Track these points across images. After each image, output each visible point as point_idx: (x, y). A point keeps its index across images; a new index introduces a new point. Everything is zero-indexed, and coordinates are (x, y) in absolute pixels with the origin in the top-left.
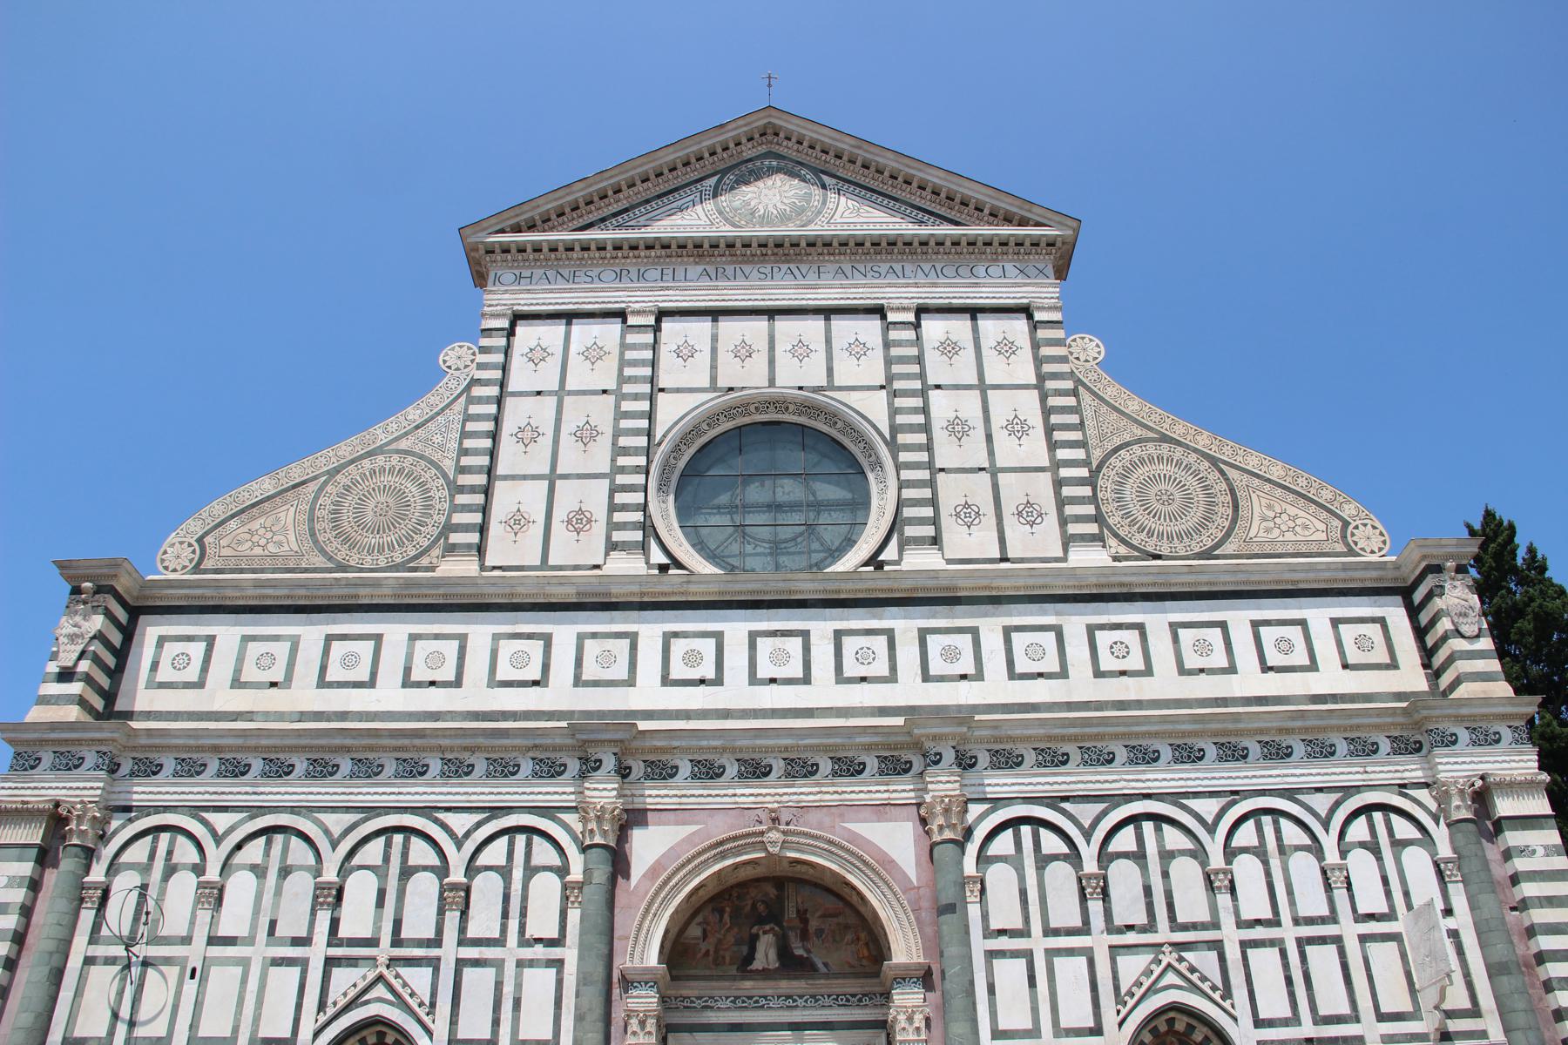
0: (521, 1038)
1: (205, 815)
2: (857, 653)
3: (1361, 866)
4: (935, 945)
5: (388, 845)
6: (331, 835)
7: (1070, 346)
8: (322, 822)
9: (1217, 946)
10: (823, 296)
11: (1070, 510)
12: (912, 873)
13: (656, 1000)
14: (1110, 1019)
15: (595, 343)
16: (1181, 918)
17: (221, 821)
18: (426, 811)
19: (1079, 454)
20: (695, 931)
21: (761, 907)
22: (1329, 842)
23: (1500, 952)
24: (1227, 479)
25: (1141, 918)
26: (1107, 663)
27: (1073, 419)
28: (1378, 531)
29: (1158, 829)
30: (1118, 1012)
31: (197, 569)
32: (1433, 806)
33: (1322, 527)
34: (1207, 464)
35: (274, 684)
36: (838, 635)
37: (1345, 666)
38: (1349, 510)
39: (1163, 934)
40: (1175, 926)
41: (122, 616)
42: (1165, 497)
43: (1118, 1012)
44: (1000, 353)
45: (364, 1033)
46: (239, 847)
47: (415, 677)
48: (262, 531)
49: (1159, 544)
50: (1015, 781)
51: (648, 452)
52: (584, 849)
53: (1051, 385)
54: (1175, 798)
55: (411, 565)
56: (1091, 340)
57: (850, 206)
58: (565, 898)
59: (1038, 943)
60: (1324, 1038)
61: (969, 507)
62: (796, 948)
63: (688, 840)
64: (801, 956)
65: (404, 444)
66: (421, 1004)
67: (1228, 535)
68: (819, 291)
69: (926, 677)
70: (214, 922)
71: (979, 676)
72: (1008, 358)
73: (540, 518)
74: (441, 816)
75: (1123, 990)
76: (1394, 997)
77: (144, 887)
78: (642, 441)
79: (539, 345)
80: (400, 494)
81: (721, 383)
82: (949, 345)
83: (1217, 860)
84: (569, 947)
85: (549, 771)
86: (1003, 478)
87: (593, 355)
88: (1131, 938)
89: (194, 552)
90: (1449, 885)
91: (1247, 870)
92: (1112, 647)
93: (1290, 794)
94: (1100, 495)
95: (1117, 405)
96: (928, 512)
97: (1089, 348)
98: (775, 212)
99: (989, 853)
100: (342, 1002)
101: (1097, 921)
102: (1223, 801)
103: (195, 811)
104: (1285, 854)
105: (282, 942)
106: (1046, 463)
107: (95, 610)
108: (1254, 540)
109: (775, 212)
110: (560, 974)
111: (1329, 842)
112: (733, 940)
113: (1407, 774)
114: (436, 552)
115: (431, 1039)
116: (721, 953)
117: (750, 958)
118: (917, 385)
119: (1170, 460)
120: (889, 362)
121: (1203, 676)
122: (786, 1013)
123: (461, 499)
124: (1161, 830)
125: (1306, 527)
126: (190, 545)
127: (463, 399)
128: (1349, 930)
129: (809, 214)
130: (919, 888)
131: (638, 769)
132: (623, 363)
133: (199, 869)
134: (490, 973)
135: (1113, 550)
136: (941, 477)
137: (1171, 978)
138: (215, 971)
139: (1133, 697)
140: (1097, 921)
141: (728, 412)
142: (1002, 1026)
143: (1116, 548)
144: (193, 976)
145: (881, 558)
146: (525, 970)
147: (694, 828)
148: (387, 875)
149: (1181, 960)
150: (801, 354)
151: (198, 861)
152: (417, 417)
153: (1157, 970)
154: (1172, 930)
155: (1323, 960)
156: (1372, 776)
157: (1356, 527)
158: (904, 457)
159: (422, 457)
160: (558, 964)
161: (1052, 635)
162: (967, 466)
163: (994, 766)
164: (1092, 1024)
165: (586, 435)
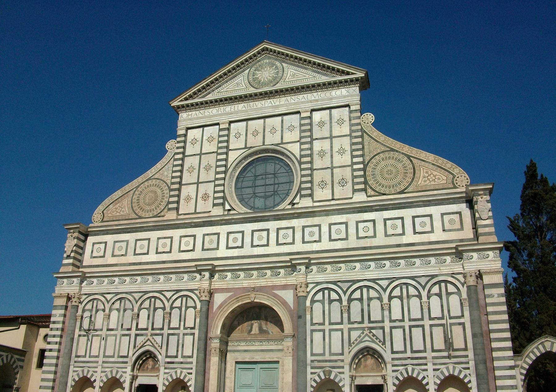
0: (184, 355)
1: (104, 295)
2: (283, 235)
3: (435, 302)
4: (296, 327)
5: (150, 302)
6: (136, 299)
7: (362, 118)
8: (133, 296)
9: (383, 328)
10: (281, 110)
11: (356, 180)
12: (292, 306)
13: (219, 344)
14: (346, 350)
15: (211, 136)
16: (372, 319)
17: (109, 297)
19: (361, 159)
21: (254, 315)
22: (424, 294)
23: (478, 330)
24: (412, 163)
25: (359, 319)
28: (466, 178)
29: (368, 291)
30: (349, 348)
31: (102, 221)
32: (462, 280)
33: (445, 178)
34: (406, 158)
35: (122, 255)
37: (444, 230)
39: (366, 324)
40: (370, 322)
41: (82, 237)
42: (389, 172)
43: (349, 348)
44: (338, 124)
45: (146, 354)
46: (113, 303)
47: (159, 251)
48: (119, 208)
49: (385, 190)
50: (323, 276)
51: (225, 172)
52: (201, 301)
54: (374, 281)
55: (158, 215)
56: (370, 115)
57: (292, 74)
58: (195, 315)
59: (327, 327)
60: (414, 357)
61: (323, 182)
62: (264, 327)
63: (230, 298)
64: (265, 330)
65: (156, 176)
66: (159, 346)
67: (410, 184)
68: (279, 108)
69: (304, 242)
70: (108, 324)
71: (320, 241)
72: (341, 125)
73: (195, 197)
74: (163, 293)
75: (352, 342)
76: (439, 343)
77: (91, 316)
78: (223, 169)
79: (194, 138)
80: (155, 192)
82: (321, 123)
83: (386, 300)
84: (196, 330)
85: (192, 278)
86: (335, 170)
88: (356, 325)
89: (101, 216)
90: (464, 307)
91: (396, 303)
92: (363, 228)
93: (412, 278)
94: (367, 173)
95: (376, 139)
96: (309, 185)
97: (370, 117)
98: (267, 80)
99: (314, 299)
100: (139, 346)
101: (345, 320)
102: (390, 281)
103: (102, 294)
104: (409, 298)
105: (124, 330)
106: (350, 164)
107: (74, 238)
108: (419, 185)
109: (267, 80)
110: (194, 337)
111: (424, 294)
112: (246, 325)
113: (455, 270)
114: (166, 210)
115: (161, 355)
116: (243, 329)
117: (251, 330)
118: (309, 139)
119: (393, 158)
120: (302, 131)
121: (393, 237)
122: (260, 347)
123: (172, 193)
124: (369, 291)
125: (439, 179)
126: (100, 214)
127: (173, 159)
128: (427, 323)
129: (278, 79)
130: (293, 310)
133: (104, 310)
134: (176, 337)
135: (369, 193)
136: (315, 172)
137: (367, 338)
138: (109, 338)
139: (368, 245)
140: (345, 320)
141: (250, 155)
142: (315, 352)
143: (370, 192)
144: (103, 340)
145: (294, 202)
146: (185, 336)
147: (231, 294)
148: (150, 310)
149: (371, 332)
150: (273, 132)
151: (104, 308)
152: (160, 167)
153: (362, 336)
154: (369, 323)
155: (417, 333)
156: (442, 271)
157: (458, 177)
158: (303, 166)
159: (161, 180)
160: (193, 334)
161: (344, 225)
162: (324, 167)
163: (318, 272)
164: (341, 352)
165: (208, 168)
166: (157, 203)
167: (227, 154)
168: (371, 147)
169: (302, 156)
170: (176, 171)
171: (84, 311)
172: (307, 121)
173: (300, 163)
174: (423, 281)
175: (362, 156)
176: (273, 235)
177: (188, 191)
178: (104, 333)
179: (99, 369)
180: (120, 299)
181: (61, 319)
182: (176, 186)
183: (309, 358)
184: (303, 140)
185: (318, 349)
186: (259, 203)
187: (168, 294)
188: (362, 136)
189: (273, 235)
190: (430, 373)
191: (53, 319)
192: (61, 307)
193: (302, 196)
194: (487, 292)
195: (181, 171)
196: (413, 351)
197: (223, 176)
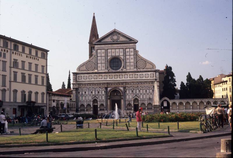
3: (148, 90)
17: (85, 88)
19: (136, 61)
22: (146, 89)
26: (135, 77)
27: (136, 58)
38: (154, 65)
47: (95, 78)
53: (135, 55)
59: (129, 94)
69: (124, 78)
73: (101, 66)
78: (107, 61)
80: (91, 65)
83: (139, 90)
87: (103, 53)
91: (141, 90)
93: (144, 86)
111: (146, 89)
120: (124, 53)
123: (96, 65)
128: (146, 94)
132: (105, 54)
136: (127, 63)
140: (132, 93)
155: (144, 96)
158: (124, 62)
166: (92, 67)
167: (107, 57)
168: (138, 59)
169: (124, 59)
172: (125, 51)
173: (123, 61)
175: (136, 60)
176: (118, 76)
177: (99, 65)
178: (85, 95)
179: (85, 104)
180: (88, 89)
181: (75, 93)
182: (96, 64)
183: (126, 100)
184: (124, 55)
185: (128, 98)
186: (115, 68)
188: (136, 56)
189: (118, 76)
190: (146, 102)
191: (73, 93)
192: (75, 91)
193: (124, 68)
195: (97, 60)
196: (144, 99)
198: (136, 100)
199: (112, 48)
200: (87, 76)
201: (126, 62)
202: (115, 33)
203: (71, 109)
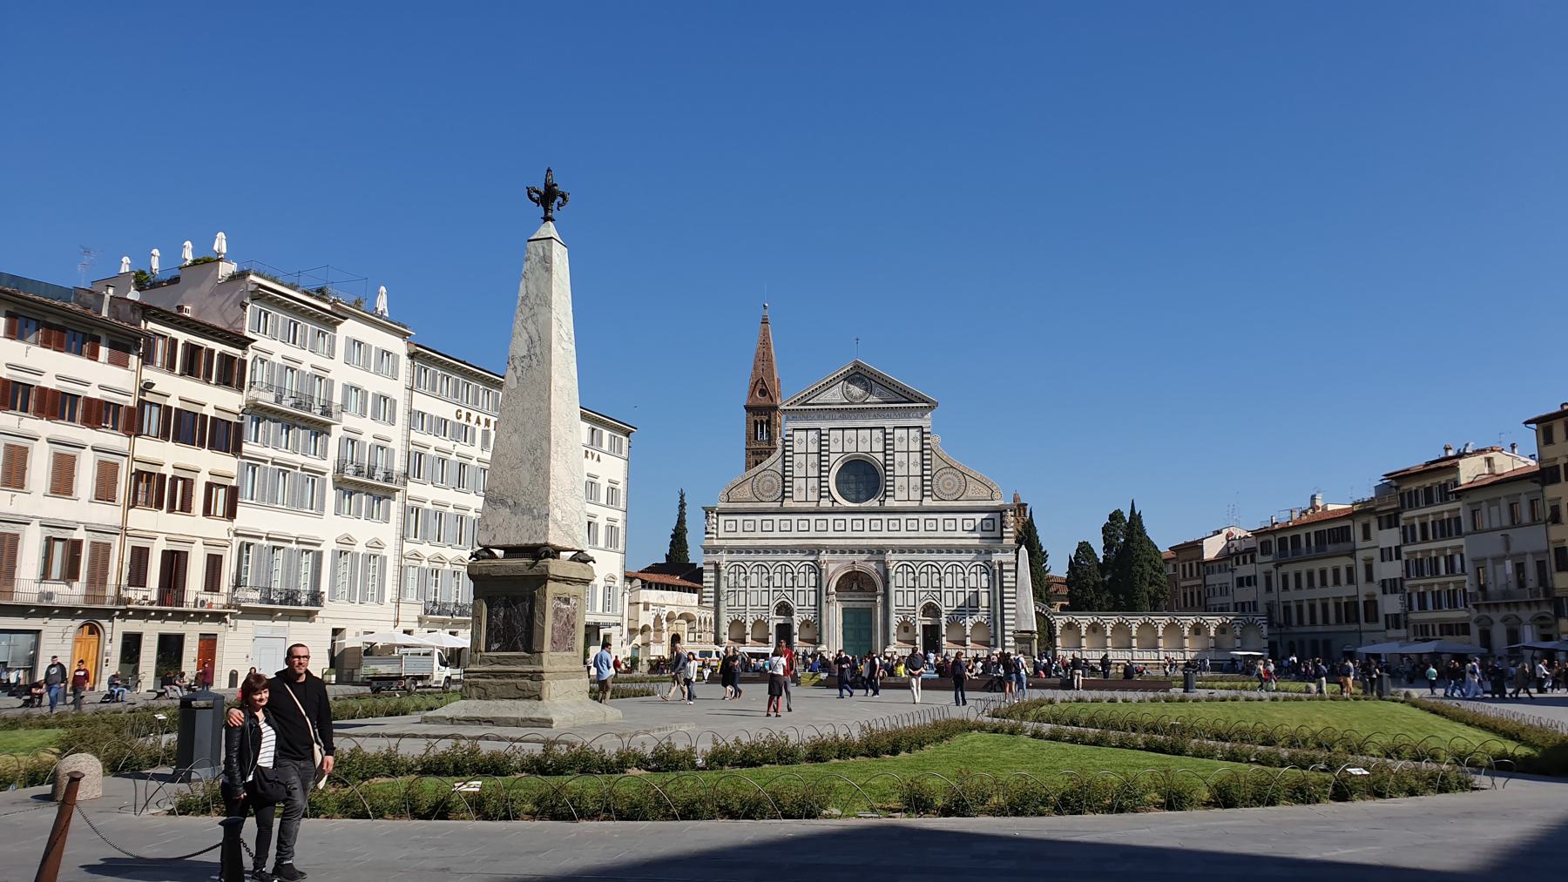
9: (940, 591)
14: (917, 604)
17: (748, 564)
18: (788, 561)
19: (929, 472)
20: (841, 582)
22: (967, 572)
27: (929, 462)
31: (728, 502)
36: (870, 520)
40: (932, 587)
54: (935, 561)
59: (905, 589)
69: (889, 530)
78: (827, 469)
81: (845, 451)
88: (923, 589)
96: (892, 488)
101: (917, 585)
118: (892, 452)
120: (885, 445)
128: (967, 590)
131: (829, 551)
133: (746, 573)
158: (888, 473)
167: (828, 456)
170: (788, 466)
171: (729, 573)
173: (885, 471)
174: (966, 564)
176: (867, 524)
179: (748, 614)
187: (795, 563)
188: (931, 454)
189: (867, 524)
191: (704, 580)
192: (711, 571)
193: (886, 496)
194: (1005, 574)
197: (827, 474)
198: (931, 611)
199: (847, 424)
200: (755, 521)
201: (894, 476)
202: (857, 373)
203: (700, 637)
